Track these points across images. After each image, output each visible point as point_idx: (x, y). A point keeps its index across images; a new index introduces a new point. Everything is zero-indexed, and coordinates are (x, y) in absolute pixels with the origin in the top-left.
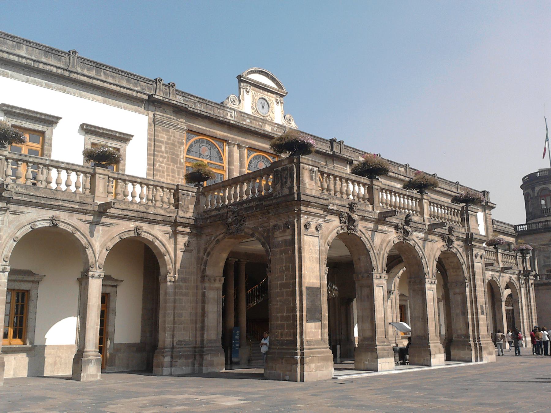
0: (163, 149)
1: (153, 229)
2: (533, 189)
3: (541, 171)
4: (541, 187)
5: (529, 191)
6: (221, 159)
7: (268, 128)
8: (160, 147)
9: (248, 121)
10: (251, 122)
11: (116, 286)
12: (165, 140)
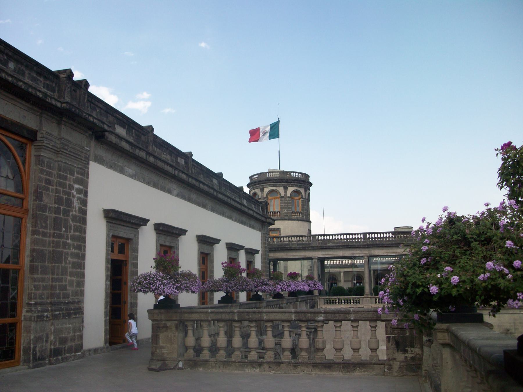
2: (262, 190)
5: (258, 191)
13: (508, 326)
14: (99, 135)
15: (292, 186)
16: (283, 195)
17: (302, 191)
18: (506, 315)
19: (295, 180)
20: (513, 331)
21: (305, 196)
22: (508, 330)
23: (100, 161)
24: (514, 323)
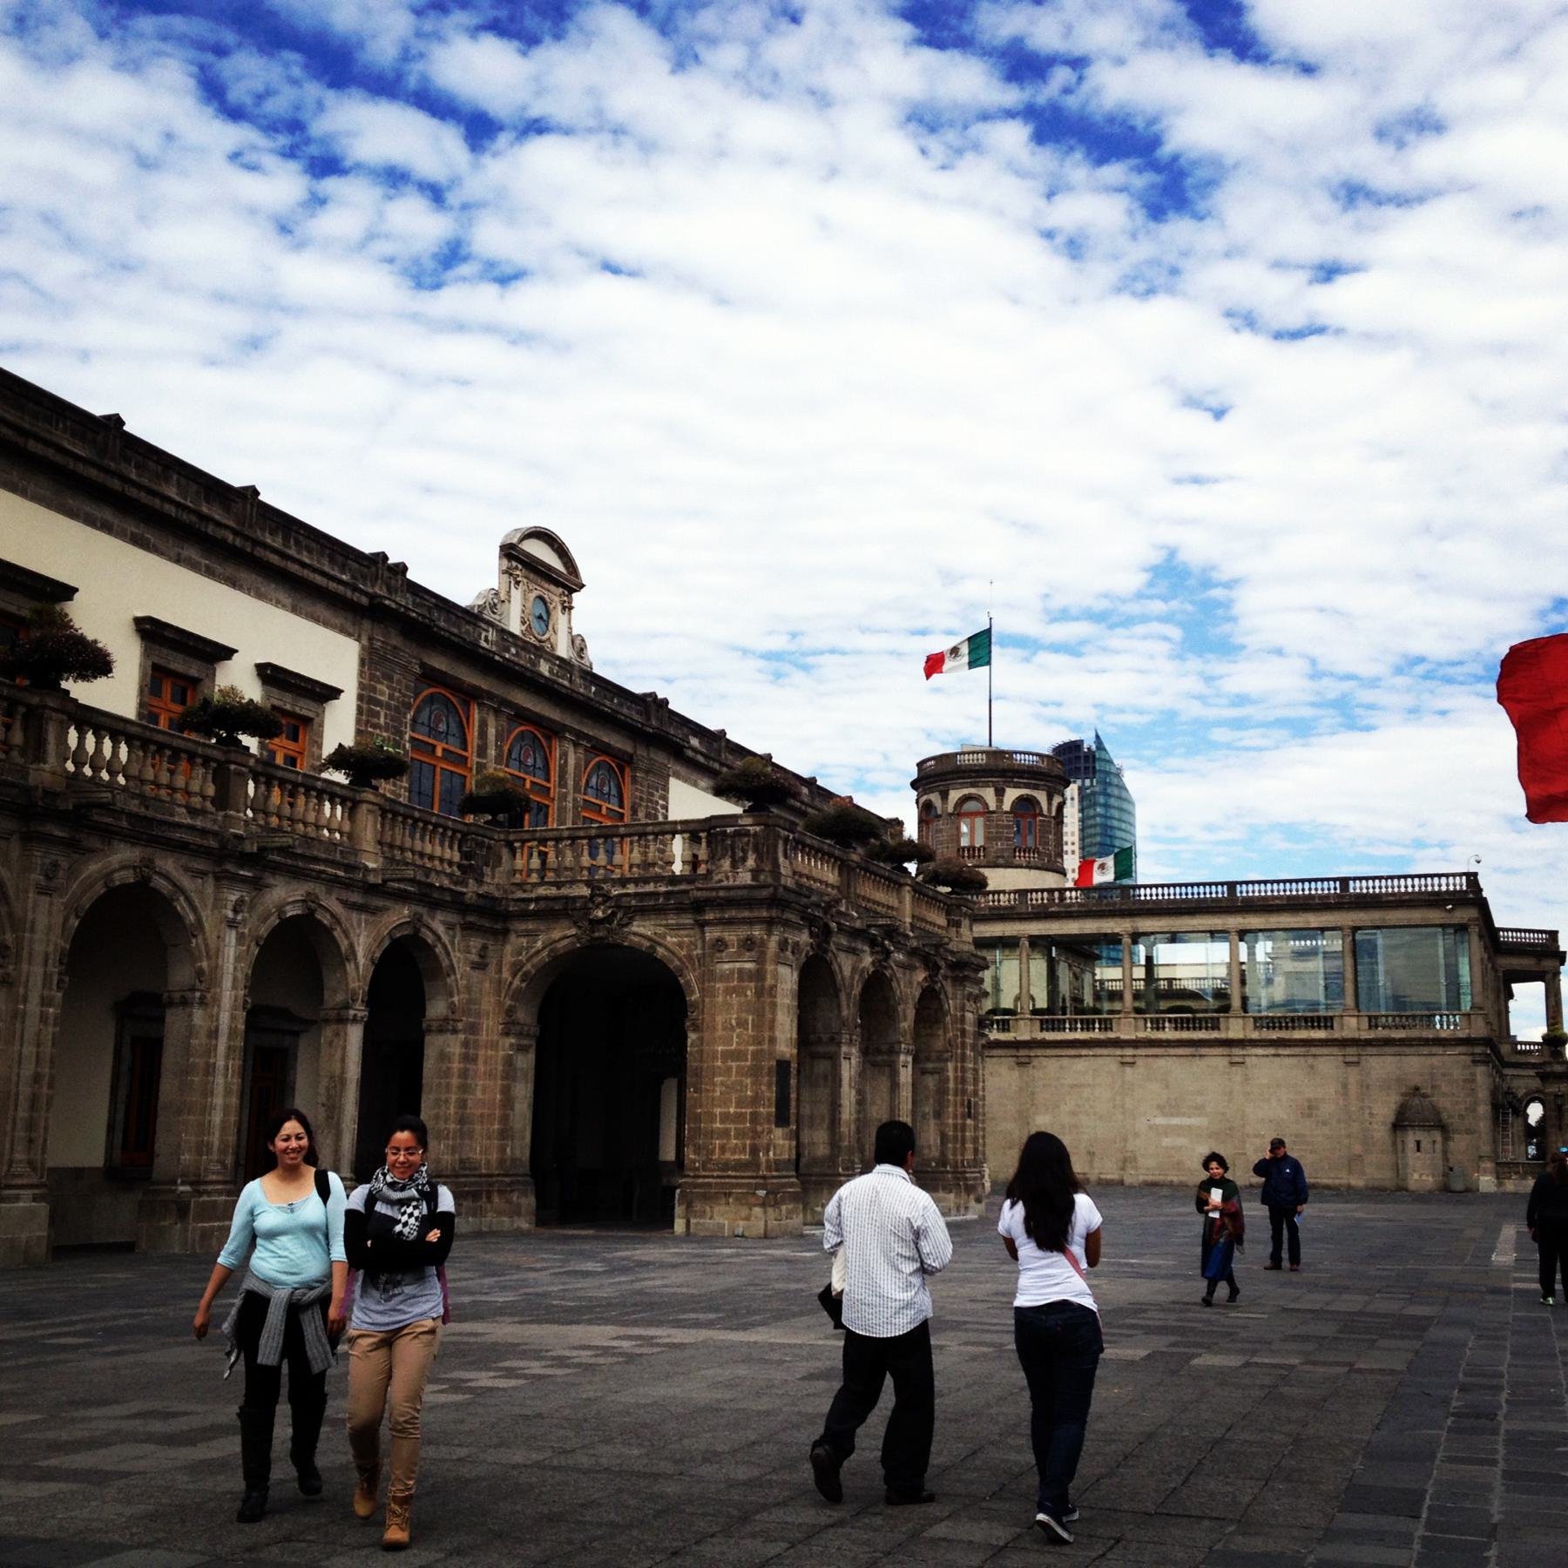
0: (382, 720)
1: (433, 918)
4: (966, 791)
5: (935, 798)
6: (464, 744)
7: (544, 668)
8: (377, 715)
9: (513, 650)
10: (517, 655)
11: (296, 1034)
12: (384, 699)
13: (1417, 1080)
14: (677, 752)
15: (1017, 786)
16: (992, 807)
17: (1041, 797)
18: (1415, 1059)
19: (1024, 772)
20: (1429, 1091)
21: (1049, 810)
22: (1417, 1089)
23: (678, 776)
24: (1432, 1074)
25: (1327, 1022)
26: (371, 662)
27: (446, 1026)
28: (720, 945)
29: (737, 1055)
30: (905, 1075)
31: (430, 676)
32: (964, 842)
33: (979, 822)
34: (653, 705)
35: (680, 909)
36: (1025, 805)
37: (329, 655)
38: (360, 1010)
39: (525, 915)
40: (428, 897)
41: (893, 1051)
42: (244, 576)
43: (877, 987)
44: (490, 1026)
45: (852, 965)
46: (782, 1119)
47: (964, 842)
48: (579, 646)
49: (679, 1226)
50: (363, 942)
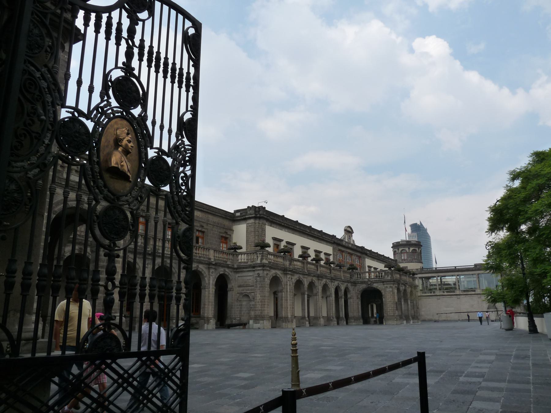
2: (398, 249)
3: (402, 241)
5: (396, 250)
14: (366, 254)
17: (417, 249)
25: (474, 291)
26: (334, 249)
27: (350, 298)
28: (387, 287)
29: (391, 301)
30: (409, 303)
31: (339, 250)
32: (403, 258)
33: (405, 254)
34: (362, 248)
35: (381, 282)
36: (414, 251)
37: (327, 249)
38: (343, 297)
39: (358, 283)
40: (348, 282)
41: (407, 300)
42: (322, 242)
43: (405, 290)
44: (355, 298)
45: (402, 288)
46: (397, 310)
47: (403, 258)
48: (354, 241)
49: (384, 323)
50: (343, 288)
